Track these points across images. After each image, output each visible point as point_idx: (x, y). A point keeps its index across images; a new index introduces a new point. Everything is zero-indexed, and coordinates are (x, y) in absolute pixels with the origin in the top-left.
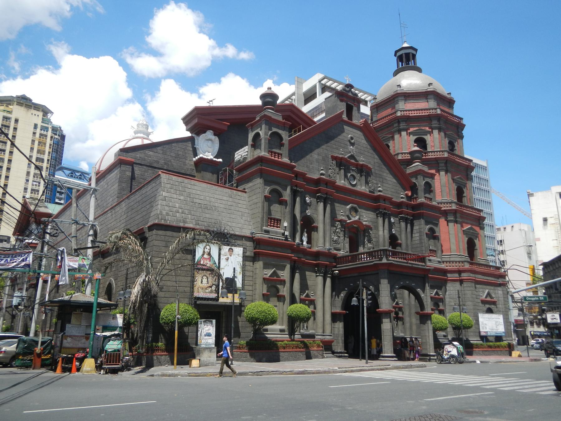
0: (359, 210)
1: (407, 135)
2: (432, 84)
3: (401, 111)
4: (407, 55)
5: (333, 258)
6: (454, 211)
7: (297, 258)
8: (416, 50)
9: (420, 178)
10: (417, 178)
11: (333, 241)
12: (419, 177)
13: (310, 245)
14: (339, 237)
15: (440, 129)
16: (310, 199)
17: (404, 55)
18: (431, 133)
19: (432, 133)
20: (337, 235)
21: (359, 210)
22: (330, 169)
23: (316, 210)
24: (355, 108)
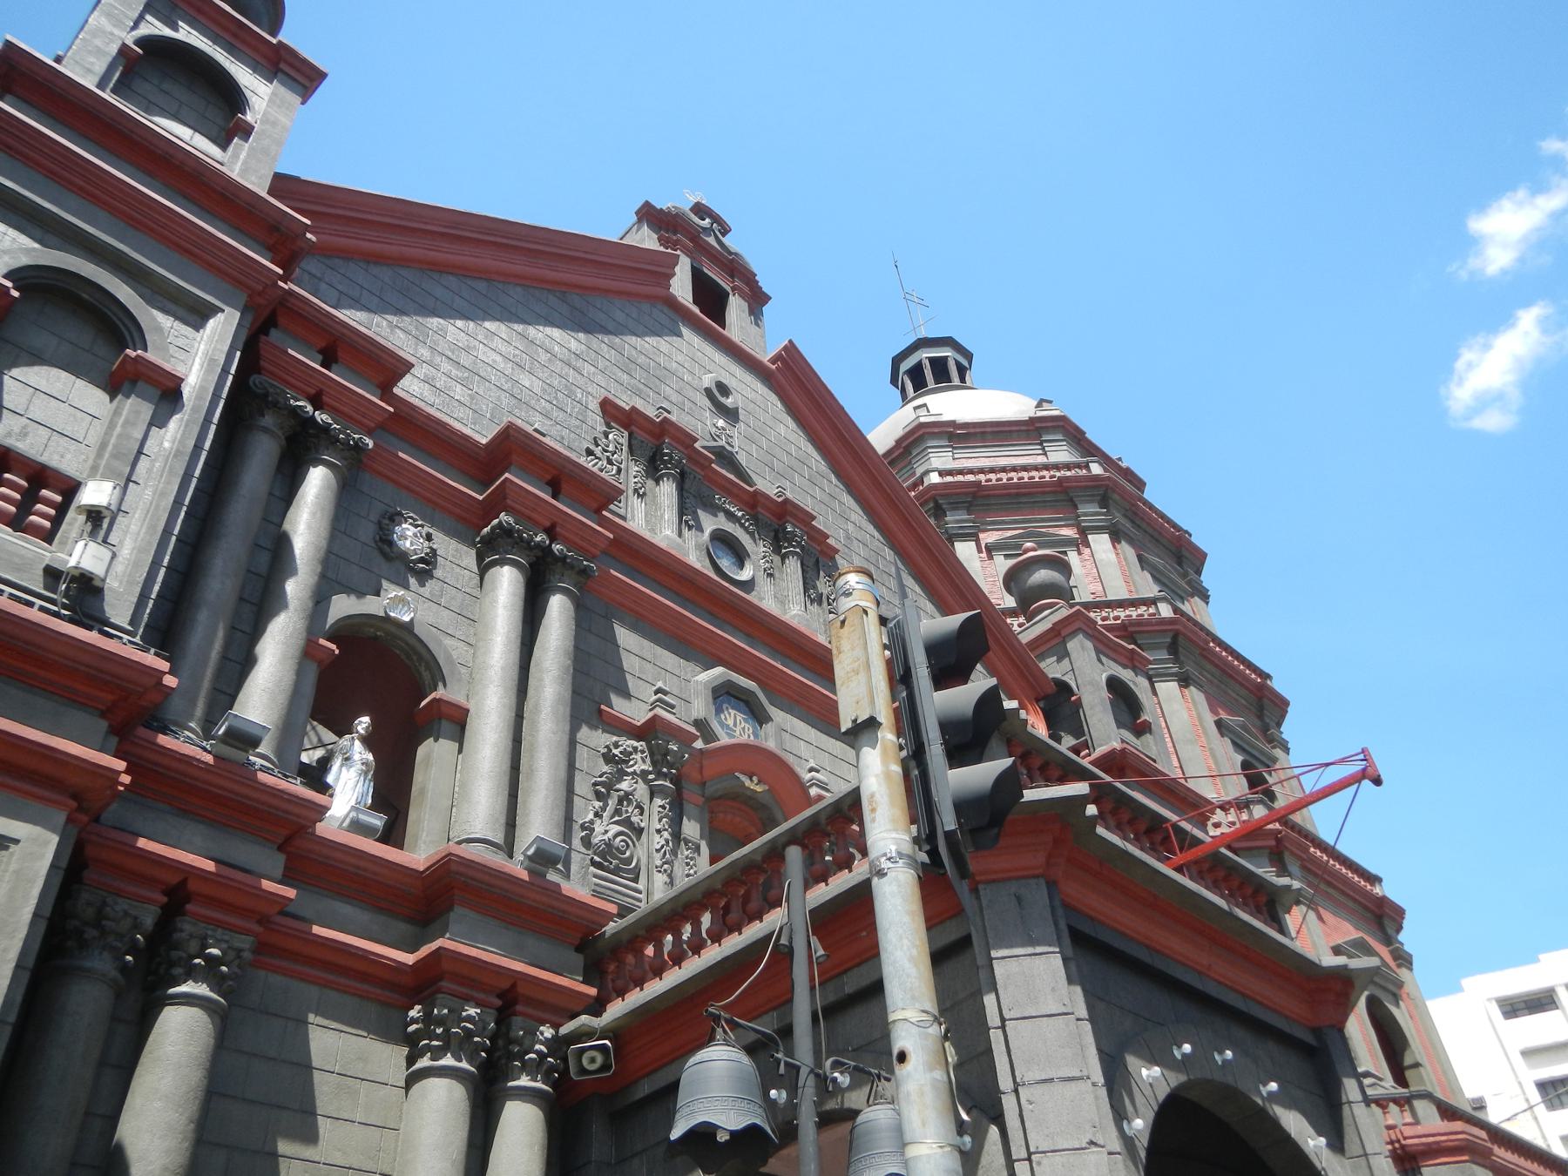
0: (774, 712)
1: (980, 551)
2: (1050, 402)
3: (942, 473)
4: (940, 367)
5: (579, 949)
6: (1273, 843)
7: (209, 866)
8: (969, 356)
9: (1080, 648)
10: (1063, 654)
11: (587, 842)
12: (1071, 645)
13: (377, 821)
14: (639, 831)
15: (1116, 536)
16: (429, 538)
17: (927, 364)
18: (1081, 543)
19: (1088, 546)
20: (617, 812)
21: (774, 712)
22: (589, 452)
23: (473, 619)
24: (736, 308)
